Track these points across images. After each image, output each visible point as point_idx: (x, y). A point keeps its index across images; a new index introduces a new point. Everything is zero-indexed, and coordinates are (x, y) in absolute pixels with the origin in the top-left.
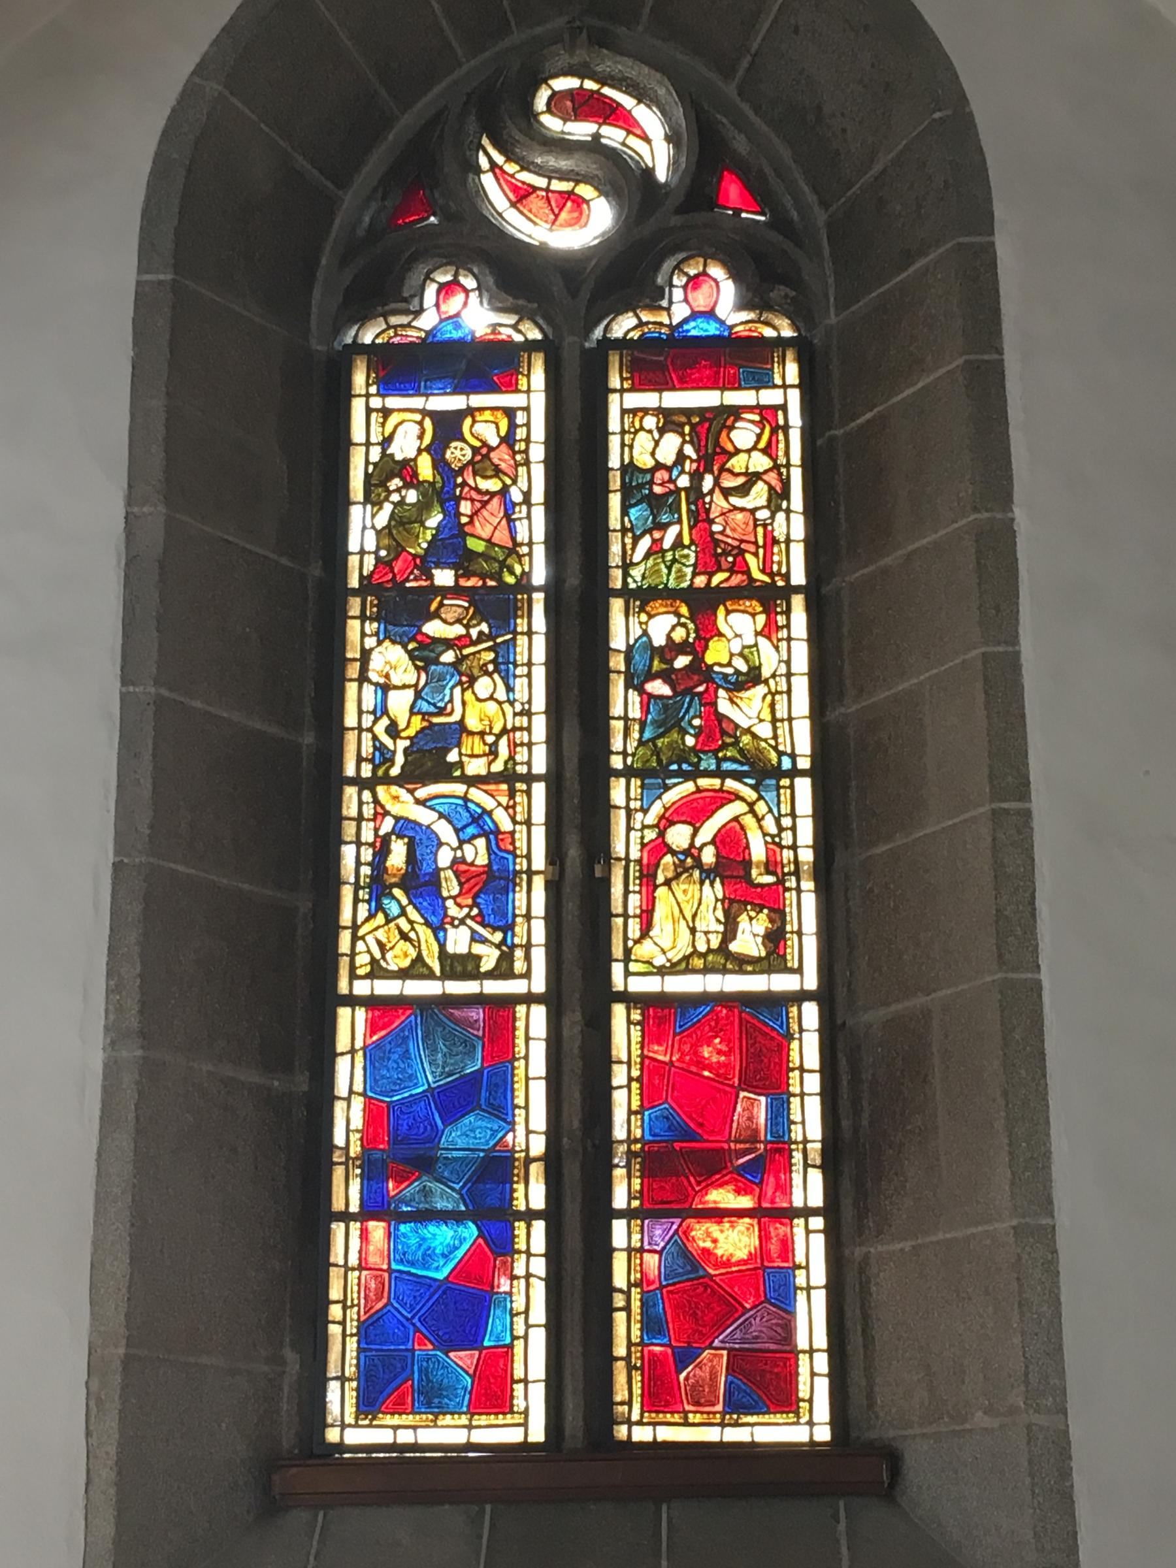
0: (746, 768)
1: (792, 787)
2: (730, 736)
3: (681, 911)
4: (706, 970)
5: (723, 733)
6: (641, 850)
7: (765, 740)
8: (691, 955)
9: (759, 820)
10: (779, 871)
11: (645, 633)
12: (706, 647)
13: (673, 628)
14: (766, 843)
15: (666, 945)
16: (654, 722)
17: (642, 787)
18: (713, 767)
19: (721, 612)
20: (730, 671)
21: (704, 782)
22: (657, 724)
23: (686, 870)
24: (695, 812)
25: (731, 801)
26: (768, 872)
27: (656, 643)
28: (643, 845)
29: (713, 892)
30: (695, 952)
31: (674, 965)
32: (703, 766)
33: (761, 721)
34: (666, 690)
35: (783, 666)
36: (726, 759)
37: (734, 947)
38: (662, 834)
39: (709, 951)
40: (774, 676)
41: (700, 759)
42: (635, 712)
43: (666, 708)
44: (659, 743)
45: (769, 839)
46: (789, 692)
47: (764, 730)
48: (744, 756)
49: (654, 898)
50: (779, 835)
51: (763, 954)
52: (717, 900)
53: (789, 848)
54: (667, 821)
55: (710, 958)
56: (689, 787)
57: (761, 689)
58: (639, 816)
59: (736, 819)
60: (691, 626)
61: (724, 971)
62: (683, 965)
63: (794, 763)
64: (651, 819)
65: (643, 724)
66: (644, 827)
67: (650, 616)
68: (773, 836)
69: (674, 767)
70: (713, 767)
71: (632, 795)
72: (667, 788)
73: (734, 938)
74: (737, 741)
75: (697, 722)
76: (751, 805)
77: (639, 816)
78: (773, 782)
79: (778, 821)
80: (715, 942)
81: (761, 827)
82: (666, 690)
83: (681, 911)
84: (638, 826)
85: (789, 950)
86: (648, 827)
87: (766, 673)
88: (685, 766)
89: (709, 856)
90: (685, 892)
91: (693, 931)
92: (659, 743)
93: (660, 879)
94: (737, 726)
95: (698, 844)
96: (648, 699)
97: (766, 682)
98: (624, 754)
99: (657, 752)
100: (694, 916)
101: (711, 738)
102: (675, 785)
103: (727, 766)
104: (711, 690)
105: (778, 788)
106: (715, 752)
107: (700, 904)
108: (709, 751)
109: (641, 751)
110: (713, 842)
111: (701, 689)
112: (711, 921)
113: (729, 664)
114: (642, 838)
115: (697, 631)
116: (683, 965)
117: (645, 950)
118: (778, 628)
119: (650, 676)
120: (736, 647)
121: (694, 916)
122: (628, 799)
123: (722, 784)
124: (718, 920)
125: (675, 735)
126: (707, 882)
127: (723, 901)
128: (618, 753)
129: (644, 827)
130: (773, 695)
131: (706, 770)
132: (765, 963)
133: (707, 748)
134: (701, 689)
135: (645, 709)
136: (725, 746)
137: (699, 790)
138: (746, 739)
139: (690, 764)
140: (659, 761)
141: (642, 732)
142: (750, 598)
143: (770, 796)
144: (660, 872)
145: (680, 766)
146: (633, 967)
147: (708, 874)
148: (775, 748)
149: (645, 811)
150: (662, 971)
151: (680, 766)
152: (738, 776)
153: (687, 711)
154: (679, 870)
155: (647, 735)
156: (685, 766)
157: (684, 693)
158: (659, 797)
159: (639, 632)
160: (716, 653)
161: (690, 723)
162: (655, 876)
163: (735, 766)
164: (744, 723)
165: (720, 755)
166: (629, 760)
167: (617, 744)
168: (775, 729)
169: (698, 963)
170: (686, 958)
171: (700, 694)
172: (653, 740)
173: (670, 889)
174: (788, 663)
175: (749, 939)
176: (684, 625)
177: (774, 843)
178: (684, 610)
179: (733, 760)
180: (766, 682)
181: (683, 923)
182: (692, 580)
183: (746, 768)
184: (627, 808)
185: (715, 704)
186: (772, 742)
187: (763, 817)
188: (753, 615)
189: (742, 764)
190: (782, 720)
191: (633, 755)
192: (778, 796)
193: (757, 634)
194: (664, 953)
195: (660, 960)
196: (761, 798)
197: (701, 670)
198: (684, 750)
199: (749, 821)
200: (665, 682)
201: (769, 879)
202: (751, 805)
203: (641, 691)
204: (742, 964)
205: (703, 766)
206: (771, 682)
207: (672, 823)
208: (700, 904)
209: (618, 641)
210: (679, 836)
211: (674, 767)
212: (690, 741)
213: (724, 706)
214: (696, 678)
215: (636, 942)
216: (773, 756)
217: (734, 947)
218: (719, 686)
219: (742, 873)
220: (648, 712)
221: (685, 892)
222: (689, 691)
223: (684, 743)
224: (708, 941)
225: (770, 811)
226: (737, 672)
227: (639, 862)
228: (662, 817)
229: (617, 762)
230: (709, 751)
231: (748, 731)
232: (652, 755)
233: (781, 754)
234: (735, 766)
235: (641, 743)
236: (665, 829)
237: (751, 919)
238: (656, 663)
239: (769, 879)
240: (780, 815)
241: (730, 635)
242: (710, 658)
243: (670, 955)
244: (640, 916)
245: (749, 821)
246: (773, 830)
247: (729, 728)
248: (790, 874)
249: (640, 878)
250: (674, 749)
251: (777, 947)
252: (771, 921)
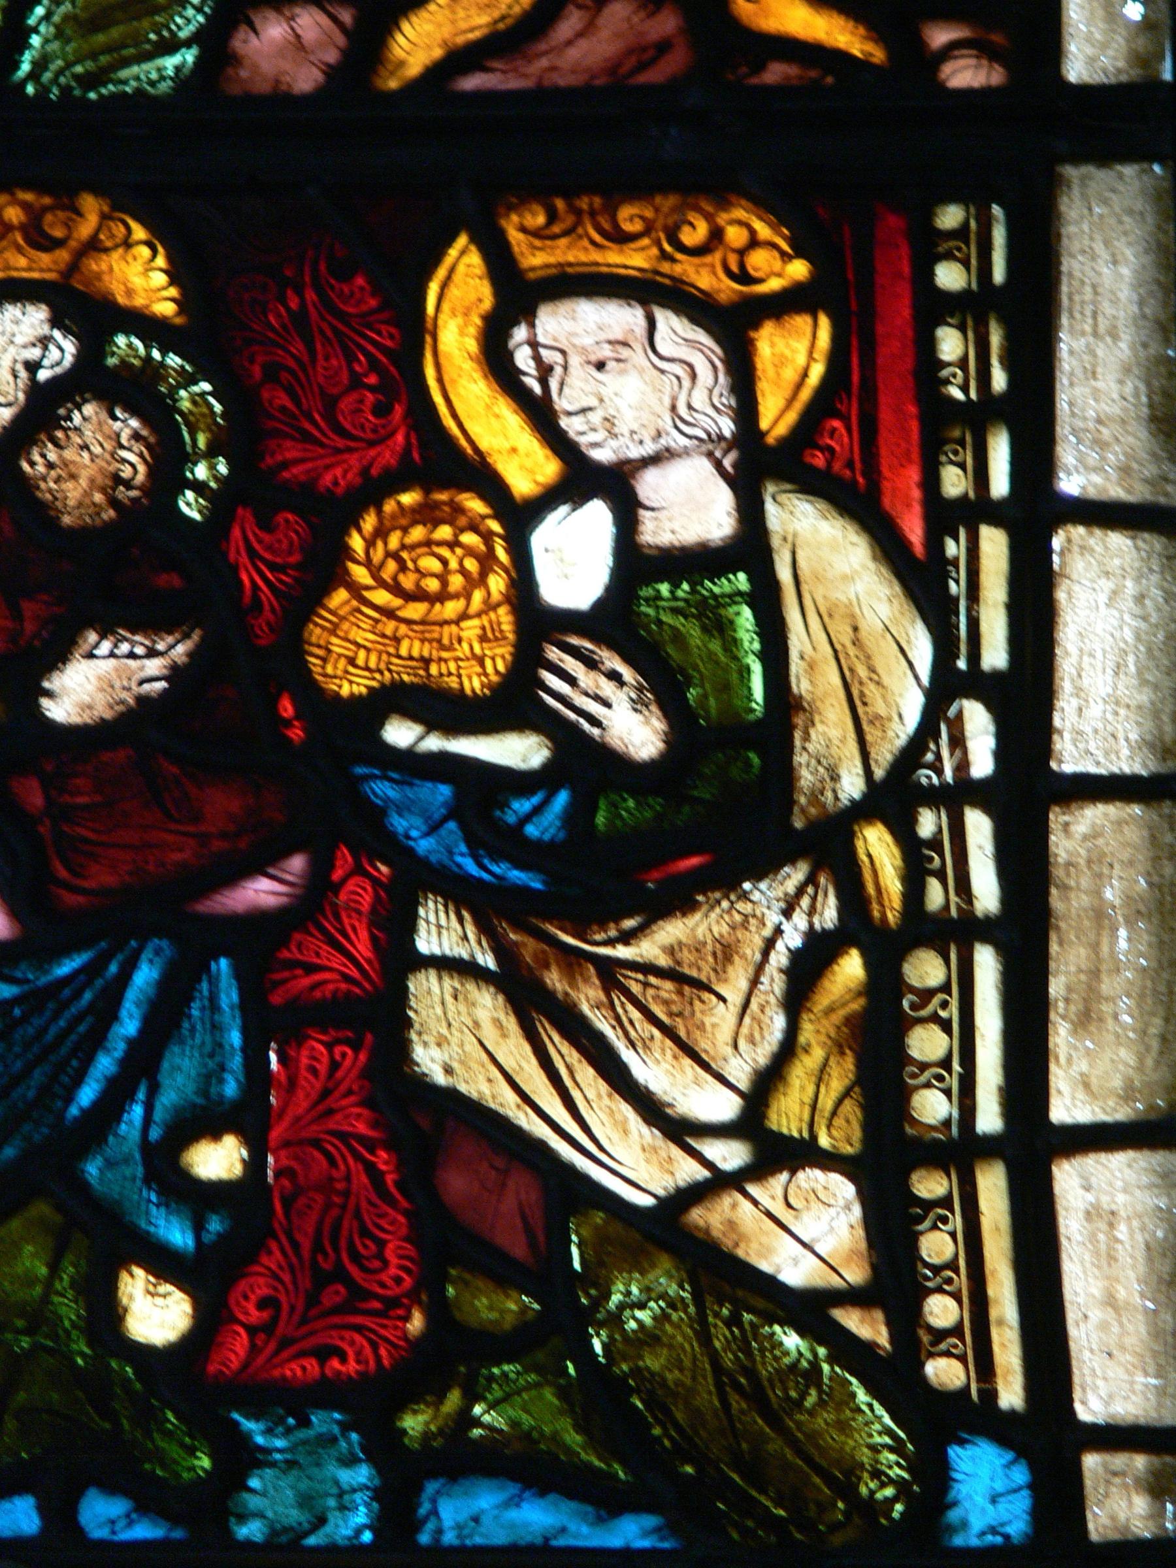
2: (505, 1274)
5: (448, 1246)
7: (810, 1309)
12: (326, 568)
19: (459, 291)
20: (518, 751)
33: (777, 1154)
35: (978, 722)
36: (462, 1457)
40: (894, 796)
41: (239, 1459)
46: (1025, 932)
47: (809, 1232)
57: (779, 911)
74: (567, 1311)
75: (217, 1160)
87: (833, 763)
94: (570, 1193)
97: (828, 846)
101: (333, 1286)
104: (359, 895)
108: (326, 1394)
111: (261, 892)
113: (514, 702)
115: (237, 438)
118: (948, 426)
120: (574, 559)
130: (886, 953)
134: (261, 892)
138: (641, 1299)
139: (147, 1499)
142: (713, 186)
145: (60, 1514)
151: (60, 1514)
153: (142, 1064)
156: (101, 1514)
157: (116, 929)
160: (397, 619)
161: (164, 1168)
164: (637, 1167)
165: (413, 1423)
168: (890, 1223)
171: (257, 937)
174: (1026, 696)
176: (135, 391)
178: (143, 277)
179: (525, 1465)
180: (828, 846)
182: (215, 42)
185: (386, 1023)
186: (867, 1327)
188: (733, 327)
189: (609, 1503)
190: (960, 1151)
193: (755, 464)
197: (264, 747)
198: (95, 1386)
206: (877, 845)
212: (156, 1314)
213: (462, 1039)
214: (222, 804)
216: (875, 1422)
218: (418, 879)
223: (107, 1315)
226: (581, 758)
230: (326, 1394)
231: (666, 1230)
233: (935, 1424)
241: (526, 466)
242: (349, 654)
247: (505, 1213)
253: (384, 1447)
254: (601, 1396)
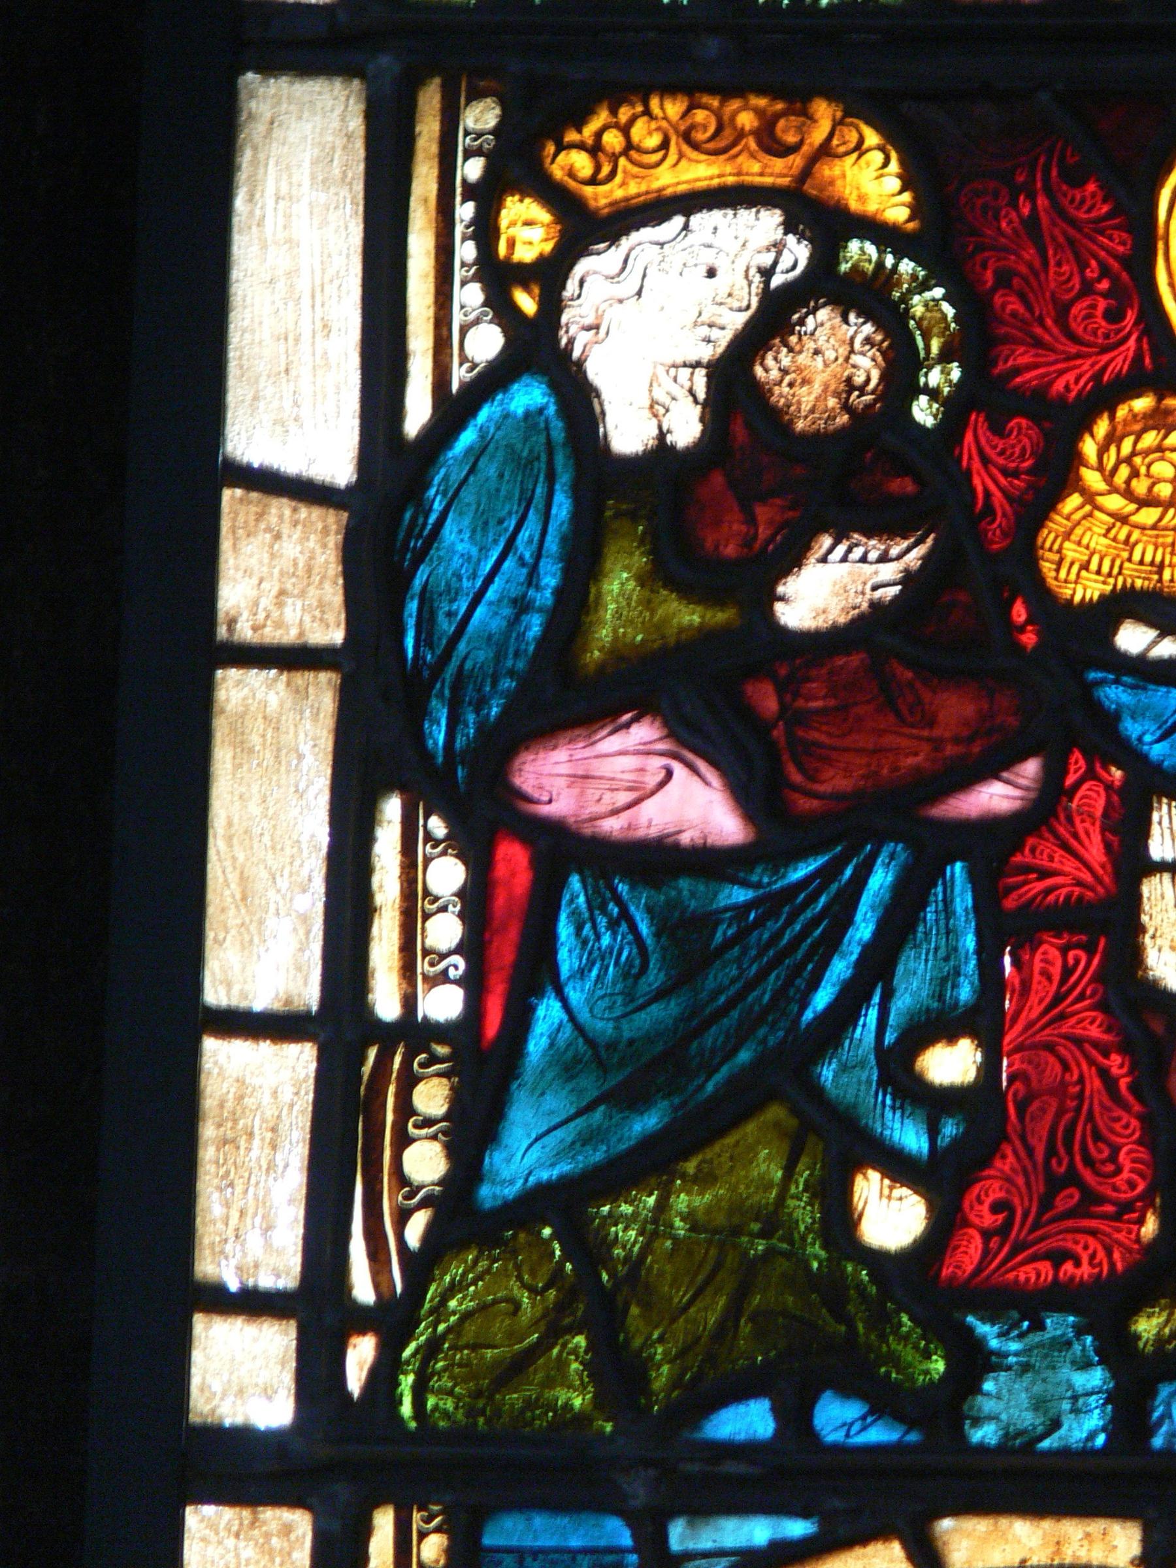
11: (538, 347)
12: (1057, 474)
13: (776, 316)
16: (584, 1055)
18: (1086, 1427)
22: (610, 1071)
27: (627, 434)
32: (1000, 1410)
34: (698, 808)
41: (973, 1363)
42: (420, 982)
43: (688, 943)
44: (625, 1223)
60: (932, 305)
65: (485, 1068)
67: (586, 228)
69: (749, 1421)
70: (1086, 1427)
75: (951, 1064)
82: (698, 808)
88: (837, 1417)
92: (625, 1223)
96: (533, 871)
98: (315, 1309)
99: (597, 1299)
101: (1067, 1189)
104: (1091, 800)
108: (1060, 1297)
111: (995, 797)
115: (973, 343)
119: (568, 693)
125: (760, 1161)
128: (253, 1304)
131: (1018, 1449)
133: (1035, 1273)
134: (995, 797)
135: (509, 955)
139: (882, 1401)
140: (618, 1372)
141: (472, 1132)
145: (795, 1417)
151: (795, 1417)
153: (877, 967)
155: (524, 1156)
156: (837, 1417)
157: (849, 832)
159: (486, 343)
166: (361, 1355)
167: (251, 1210)
171: (992, 842)
172: (563, 1203)
176: (870, 297)
178: (873, 182)
191: (392, 1321)
198: (831, 1290)
200: (693, 738)
203: (483, 809)
205: (1000, 1410)
209: (291, 390)
211: (749, 1421)
212: (891, 1217)
214: (955, 709)
220: (537, 972)
222: (902, 813)
223: (840, 1219)
229: (242, 1376)
230: (1060, 1297)
232: (554, 1328)
235: (454, 1200)
238: (618, 585)
250: (750, 1274)
253: (1116, 1350)
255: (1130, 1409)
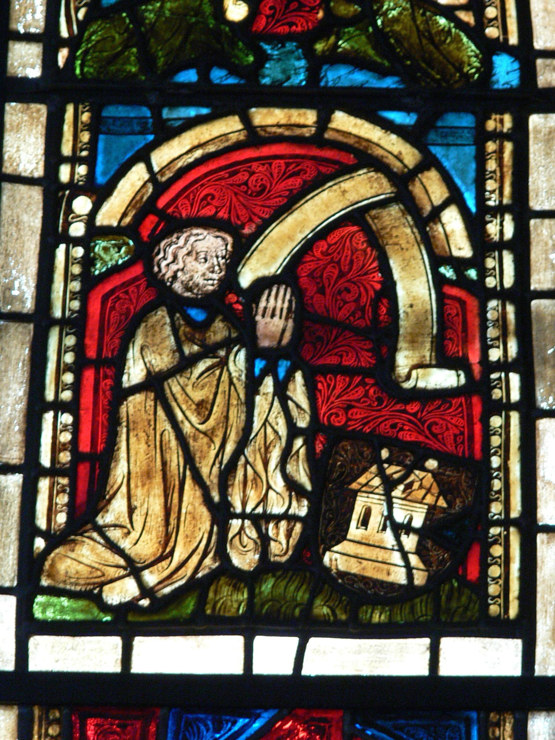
0: (390, 83)
1: (520, 136)
3: (189, 459)
4: (249, 626)
6: (83, 295)
8: (213, 576)
9: (425, 221)
10: (474, 358)
14: (439, 282)
15: (145, 547)
17: (95, 128)
18: (299, 79)
21: (267, 117)
23: (208, 351)
24: (240, 198)
25: (347, 170)
26: (443, 360)
28: (89, 281)
29: (278, 413)
30: (225, 570)
31: (161, 604)
32: (271, 73)
36: (334, 58)
37: (336, 559)
38: (145, 256)
39: (265, 565)
41: (263, 58)
45: (448, 272)
48: (387, 51)
49: (114, 422)
50: (477, 261)
51: (420, 579)
52: (293, 431)
53: (502, 294)
54: (157, 219)
55: (267, 587)
56: (230, 127)
58: (82, 205)
59: (357, 217)
61: (305, 627)
62: (190, 605)
63: (528, 72)
64: (111, 213)
66: (94, 232)
68: (460, 265)
69: (189, 76)
70: (299, 79)
71: (66, 149)
72: (166, 133)
73: (341, 535)
76: (402, 184)
77: (82, 205)
78: (467, 121)
79: (475, 226)
80: (281, 543)
81: (427, 241)
83: (189, 459)
84: (77, 230)
85: (495, 571)
86: (107, 232)
88: (218, 75)
89: (273, 320)
90: (203, 408)
91: (221, 513)
93: (135, 372)
95: (246, 278)
98: (49, 39)
100: (227, 474)
102: (190, 124)
103: (338, 76)
105: (481, 136)
106: (306, 42)
107: (244, 441)
108: (291, 37)
109: (96, 34)
110: (289, 276)
112: (273, 490)
114: (88, 262)
116: (190, 605)
117: (83, 559)
121: (227, 474)
122: (53, 157)
123: (323, 122)
124: (292, 485)
126: (268, 384)
127: (309, 435)
128: (28, 38)
129: (94, 232)
131: (277, 85)
132: (422, 609)
133: (283, 29)
136: (333, 25)
137: (254, 136)
139: (233, 71)
140: (147, 61)
143: (457, 159)
144: (133, 353)
145: (204, 75)
146: (44, 608)
147: (268, 359)
148: (476, 33)
149: (101, 193)
150: (127, 623)
151: (204, 75)
152: (365, 105)
154: (190, 349)
156: (218, 75)
158: (143, 156)
162: (119, 364)
163: (359, 78)
165: (319, 47)
166: (63, 55)
169: (234, 601)
170: (197, 586)
173: (163, 400)
175: (380, 539)
177: (462, 281)
181: (191, 495)
183: (390, 83)
184: (49, 184)
186: (467, 17)
187: (436, 213)
189: (383, 73)
191: (73, 43)
192: (481, 158)
194: (134, 568)
195: (122, 592)
196: (429, 162)
198: (217, 34)
199: (395, 223)
201: (445, 379)
202: (402, 184)
204: (361, 608)
205: (271, 73)
207: (175, 225)
208: (244, 441)
210: (194, 258)
211: (189, 76)
215: (56, 539)
217: (336, 559)
219: (366, 360)
221: (203, 408)
224: (264, 541)
225: (455, 198)
227: (75, 324)
228: (143, 208)
230: (291, 37)
232: (126, 46)
233: (490, 48)
234: (359, 78)
236: (156, 239)
237: (389, 484)
239: (445, 379)
240: (483, 208)
243: (151, 578)
244: (70, 471)
245: (395, 223)
246: (462, 248)
248: (504, 366)
249: (77, 368)
250: (190, 28)
251: (461, 561)
252: (445, 488)
253: (309, 54)
254: (380, 39)
255: (314, 74)
